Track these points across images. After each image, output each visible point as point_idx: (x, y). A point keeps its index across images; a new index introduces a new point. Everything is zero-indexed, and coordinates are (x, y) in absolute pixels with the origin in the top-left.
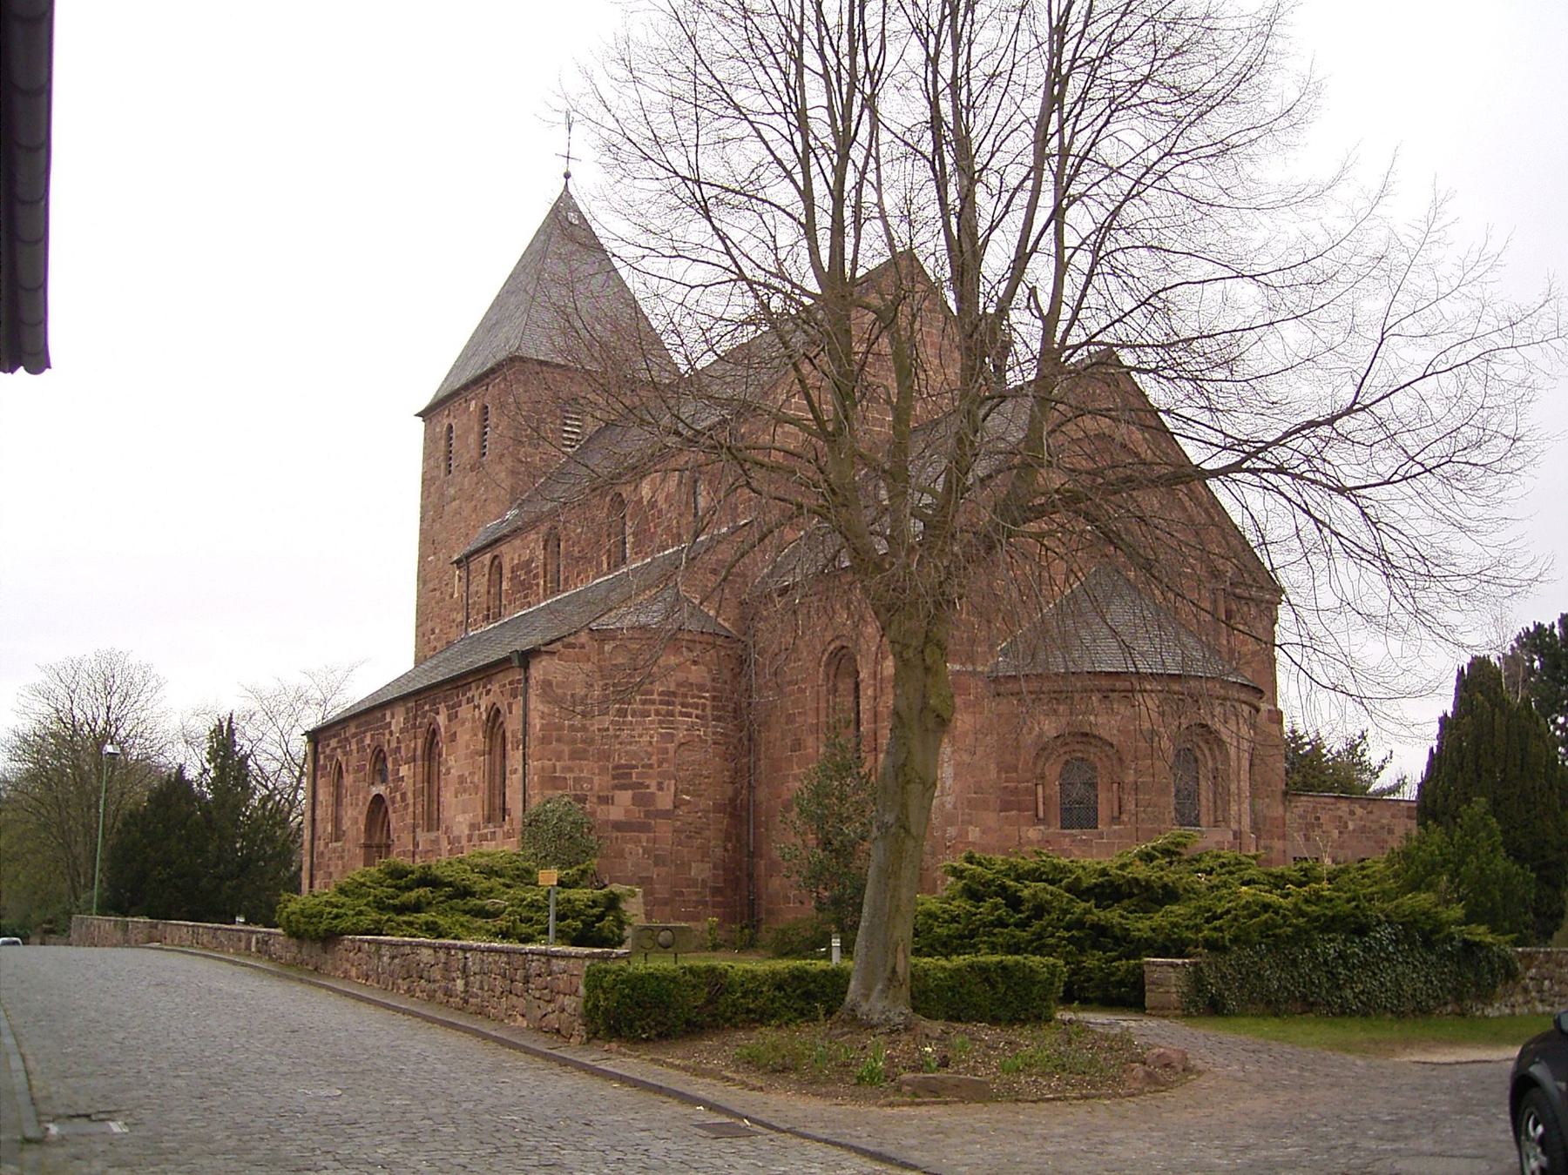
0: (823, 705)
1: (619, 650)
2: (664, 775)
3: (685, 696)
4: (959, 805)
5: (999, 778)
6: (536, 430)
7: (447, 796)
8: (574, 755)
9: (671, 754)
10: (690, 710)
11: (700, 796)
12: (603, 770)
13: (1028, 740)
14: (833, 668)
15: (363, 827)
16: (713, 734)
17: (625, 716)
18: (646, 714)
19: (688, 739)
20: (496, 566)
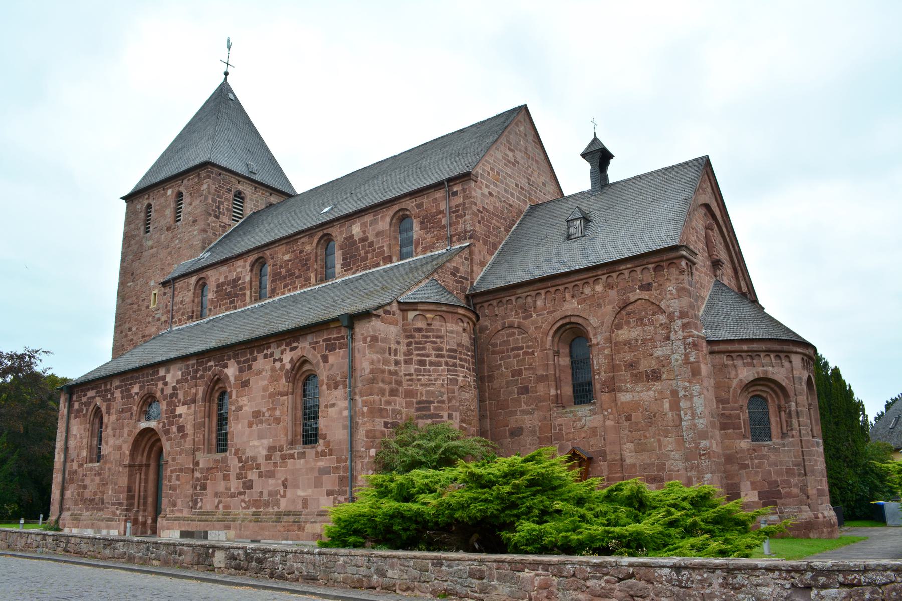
0: (551, 362)
1: (420, 316)
5: (718, 407)
6: (219, 208)
7: (237, 429)
8: (394, 392)
11: (470, 424)
12: (409, 405)
13: (735, 382)
14: (556, 339)
15: (127, 453)
16: (474, 380)
17: (425, 365)
18: (439, 364)
19: (464, 383)
20: (202, 285)
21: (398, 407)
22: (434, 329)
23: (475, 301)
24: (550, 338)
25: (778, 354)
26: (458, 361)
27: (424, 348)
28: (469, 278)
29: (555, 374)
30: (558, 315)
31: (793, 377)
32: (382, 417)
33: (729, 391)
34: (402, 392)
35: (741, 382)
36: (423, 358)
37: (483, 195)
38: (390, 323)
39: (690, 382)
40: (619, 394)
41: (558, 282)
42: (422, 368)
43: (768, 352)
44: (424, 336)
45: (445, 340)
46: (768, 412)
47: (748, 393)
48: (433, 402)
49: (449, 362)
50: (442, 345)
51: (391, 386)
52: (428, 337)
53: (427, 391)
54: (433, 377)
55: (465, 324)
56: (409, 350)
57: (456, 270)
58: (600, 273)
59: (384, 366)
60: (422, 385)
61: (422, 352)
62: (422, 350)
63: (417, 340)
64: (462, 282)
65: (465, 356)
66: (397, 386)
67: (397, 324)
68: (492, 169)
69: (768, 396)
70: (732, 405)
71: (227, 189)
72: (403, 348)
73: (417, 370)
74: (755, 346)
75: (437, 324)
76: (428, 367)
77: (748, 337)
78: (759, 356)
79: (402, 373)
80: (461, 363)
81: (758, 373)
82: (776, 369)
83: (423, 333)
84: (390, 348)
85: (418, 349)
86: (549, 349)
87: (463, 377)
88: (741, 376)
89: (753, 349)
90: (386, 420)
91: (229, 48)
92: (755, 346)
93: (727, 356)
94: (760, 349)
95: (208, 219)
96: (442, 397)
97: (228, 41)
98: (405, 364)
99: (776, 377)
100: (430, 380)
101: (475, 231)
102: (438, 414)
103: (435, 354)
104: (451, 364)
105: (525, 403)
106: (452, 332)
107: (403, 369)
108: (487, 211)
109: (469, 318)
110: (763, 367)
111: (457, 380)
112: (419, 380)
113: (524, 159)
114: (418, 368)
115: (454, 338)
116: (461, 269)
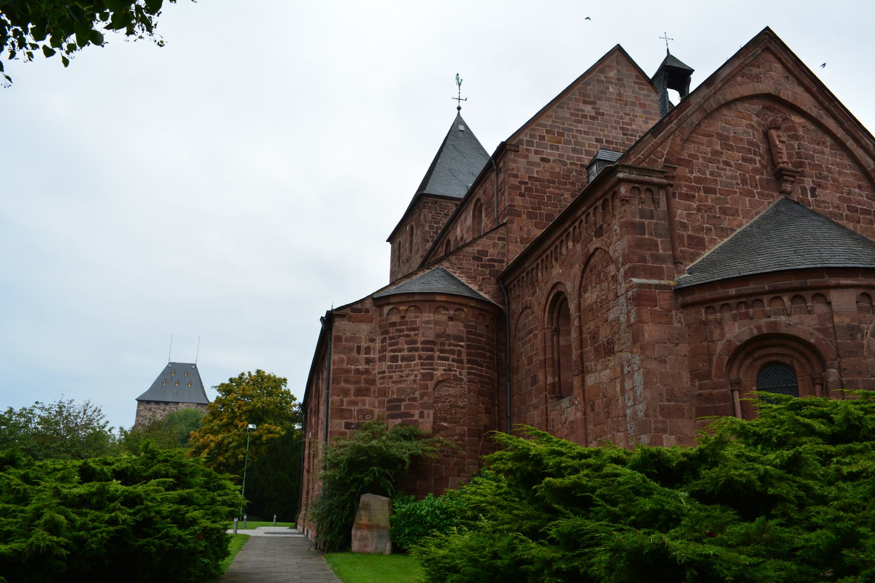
0: (548, 344)
1: (395, 311)
2: (424, 406)
3: (443, 344)
4: (651, 412)
5: (693, 386)
8: (360, 392)
9: (430, 390)
10: (447, 355)
12: (381, 404)
13: (720, 346)
14: (555, 315)
16: (469, 373)
17: (397, 361)
18: (412, 359)
19: (445, 378)
21: (367, 407)
22: (407, 321)
23: (506, 284)
24: (547, 315)
25: (797, 294)
26: (437, 354)
27: (397, 344)
28: (506, 259)
29: (553, 358)
30: (549, 286)
31: (834, 327)
32: (342, 418)
33: (711, 361)
34: (374, 391)
35: (730, 345)
36: (396, 354)
37: (530, 163)
38: (361, 321)
39: (632, 352)
40: (587, 377)
41: (546, 245)
42: (394, 364)
43: (776, 294)
44: (398, 330)
45: (420, 332)
46: (797, 387)
47: (755, 360)
48: (404, 400)
49: (423, 356)
50: (416, 338)
51: (357, 386)
52: (401, 331)
54: (404, 374)
55: (452, 312)
56: (382, 347)
57: (484, 253)
58: (567, 225)
59: (349, 366)
60: (393, 382)
61: (394, 348)
62: (394, 346)
63: (391, 335)
64: (494, 265)
65: (452, 347)
67: (371, 322)
68: (548, 132)
69: (795, 362)
70: (715, 380)
71: (444, 214)
72: (378, 345)
73: (390, 367)
74: (751, 287)
75: (411, 316)
76: (400, 363)
77: (738, 275)
78: (761, 301)
79: (376, 372)
80: (442, 355)
81: (759, 328)
82: (794, 319)
83: (397, 328)
84: (359, 348)
85: (391, 345)
86: (547, 328)
87: (444, 370)
88: (728, 336)
89: (747, 292)
91: (460, 84)
92: (751, 287)
93: (707, 308)
94: (760, 290)
95: (426, 245)
97: (458, 79)
98: (379, 362)
99: (794, 332)
100: (401, 377)
101: (515, 206)
102: (408, 413)
103: (408, 348)
104: (424, 357)
105: (535, 396)
106: (428, 322)
107: (377, 368)
108: (537, 179)
110: (769, 317)
112: (391, 377)
114: (390, 365)
115: (431, 328)
116: (491, 251)
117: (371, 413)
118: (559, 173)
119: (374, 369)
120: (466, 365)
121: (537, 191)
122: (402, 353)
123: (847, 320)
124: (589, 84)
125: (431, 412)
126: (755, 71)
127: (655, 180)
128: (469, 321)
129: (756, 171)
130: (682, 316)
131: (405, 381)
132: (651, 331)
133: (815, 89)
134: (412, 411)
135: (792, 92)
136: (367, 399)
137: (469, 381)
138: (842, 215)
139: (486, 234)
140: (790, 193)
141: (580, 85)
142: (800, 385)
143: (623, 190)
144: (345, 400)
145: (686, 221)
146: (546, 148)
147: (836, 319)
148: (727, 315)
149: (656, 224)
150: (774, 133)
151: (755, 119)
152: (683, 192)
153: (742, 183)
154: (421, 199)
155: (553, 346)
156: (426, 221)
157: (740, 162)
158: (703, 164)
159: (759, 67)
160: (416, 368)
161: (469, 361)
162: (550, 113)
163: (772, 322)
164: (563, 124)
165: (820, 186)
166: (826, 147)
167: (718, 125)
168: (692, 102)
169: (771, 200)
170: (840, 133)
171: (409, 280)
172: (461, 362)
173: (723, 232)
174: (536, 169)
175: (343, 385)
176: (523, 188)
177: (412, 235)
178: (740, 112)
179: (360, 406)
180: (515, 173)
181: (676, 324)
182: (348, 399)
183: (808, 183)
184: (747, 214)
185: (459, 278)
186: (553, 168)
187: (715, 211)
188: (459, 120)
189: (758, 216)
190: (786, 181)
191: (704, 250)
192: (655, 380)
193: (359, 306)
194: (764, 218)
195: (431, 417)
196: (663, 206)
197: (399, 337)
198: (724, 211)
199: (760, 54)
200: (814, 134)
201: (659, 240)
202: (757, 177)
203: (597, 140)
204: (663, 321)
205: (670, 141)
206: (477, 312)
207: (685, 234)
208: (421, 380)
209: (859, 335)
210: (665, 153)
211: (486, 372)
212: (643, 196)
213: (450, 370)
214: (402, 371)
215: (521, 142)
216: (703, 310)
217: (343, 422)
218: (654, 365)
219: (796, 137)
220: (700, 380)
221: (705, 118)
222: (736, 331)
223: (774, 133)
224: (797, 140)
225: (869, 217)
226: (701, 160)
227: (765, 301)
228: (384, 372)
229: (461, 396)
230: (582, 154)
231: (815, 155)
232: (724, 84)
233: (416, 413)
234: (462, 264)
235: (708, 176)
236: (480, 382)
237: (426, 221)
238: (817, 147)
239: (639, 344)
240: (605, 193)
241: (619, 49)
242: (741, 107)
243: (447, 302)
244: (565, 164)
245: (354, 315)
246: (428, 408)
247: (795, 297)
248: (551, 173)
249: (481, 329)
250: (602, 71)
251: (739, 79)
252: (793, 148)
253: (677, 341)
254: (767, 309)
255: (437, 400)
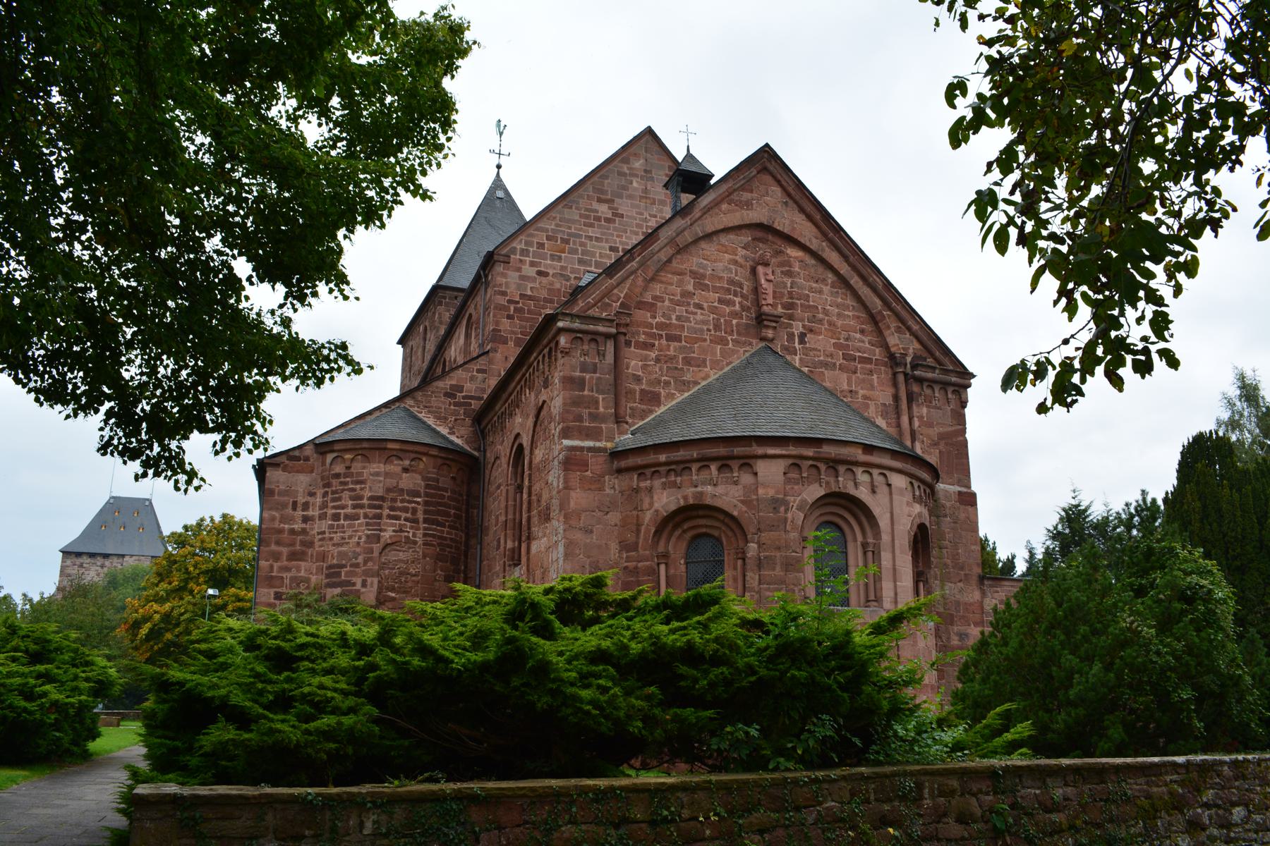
1: (339, 459)
2: (367, 573)
3: (394, 500)
8: (294, 556)
9: (376, 554)
10: (398, 513)
12: (320, 570)
16: (425, 535)
17: (339, 520)
18: (356, 517)
19: (394, 540)
21: (302, 574)
26: (386, 512)
27: (339, 499)
29: (514, 519)
32: (272, 586)
33: (638, 531)
34: (312, 555)
37: (523, 278)
38: (298, 472)
47: (684, 532)
48: (344, 566)
50: (362, 493)
52: (345, 483)
53: (339, 553)
54: (346, 535)
56: (323, 502)
57: (459, 388)
60: (334, 545)
66: (304, 549)
67: (312, 472)
69: (723, 535)
72: (319, 500)
73: (331, 527)
75: (357, 467)
76: (342, 522)
79: (315, 532)
81: (685, 498)
84: (295, 504)
85: (334, 500)
87: (394, 531)
88: (657, 505)
89: (676, 459)
90: (280, 590)
92: (681, 454)
96: (356, 559)
100: (343, 538)
101: (500, 331)
102: (349, 581)
104: (370, 515)
106: (377, 474)
108: (530, 298)
109: (416, 452)
111: (378, 537)
112: (331, 539)
113: (638, 207)
115: (380, 482)
116: (468, 386)
117: (307, 580)
118: (559, 290)
119: (312, 529)
120: (422, 525)
121: (530, 312)
122: (345, 511)
123: (771, 493)
124: (607, 177)
125: (376, 580)
126: (746, 196)
127: (601, 329)
128: (429, 473)
129: (734, 315)
130: (616, 481)
131: (348, 543)
132: (578, 498)
133: (818, 217)
134: (354, 580)
135: (790, 220)
136: (303, 564)
137: (424, 544)
138: (835, 364)
139: (461, 366)
140: (772, 340)
141: (596, 178)
142: (726, 559)
143: (563, 340)
144: (276, 565)
145: (640, 373)
146: (546, 259)
147: (761, 491)
148: (657, 483)
149: (599, 379)
150: (760, 269)
151: (742, 252)
152: (641, 340)
153: (715, 329)
154: (436, 291)
155: (515, 505)
156: (441, 323)
157: (716, 304)
158: (669, 307)
159: (752, 191)
160: (360, 529)
161: (425, 521)
162: (553, 214)
163: (698, 493)
164: (570, 228)
165: (811, 331)
166: (827, 285)
167: (694, 261)
168: (661, 235)
169: (748, 348)
170: (844, 269)
171: (362, 421)
172: (415, 521)
173: (684, 385)
174: (530, 285)
175: (274, 547)
176: (512, 308)
177: (425, 339)
178: (723, 245)
179: (293, 573)
180: (503, 289)
181: (608, 491)
182: (279, 564)
183: (797, 328)
184: (716, 365)
185: (426, 419)
186: (552, 284)
187: (678, 362)
188: (498, 184)
189: (730, 367)
190: (767, 327)
191: (659, 405)
192: (577, 552)
193: (297, 453)
194: (734, 370)
195: (376, 586)
196: (610, 358)
197: (343, 491)
198: (687, 361)
199: (755, 176)
200: (812, 270)
201: (601, 397)
202: (734, 322)
203: (612, 249)
204: (593, 487)
205: (629, 281)
206: (440, 461)
207: (637, 388)
208: (366, 543)
209: (782, 509)
210: (622, 296)
211: (448, 533)
212: (586, 347)
213: (401, 531)
214: (344, 532)
215: (514, 251)
216: (636, 476)
217: (272, 591)
218: (578, 536)
219: (789, 274)
220: (627, 552)
221: (679, 252)
222: (665, 500)
223: (760, 269)
224: (791, 277)
225: (869, 366)
226: (667, 303)
227: (693, 469)
228: (324, 533)
229: (413, 562)
230: (591, 266)
231: (811, 294)
232: (705, 213)
233: (359, 581)
234: (429, 402)
235: (674, 321)
236: (439, 544)
237: (441, 323)
238: (814, 285)
239: (563, 512)
240: (550, 342)
241: (649, 132)
242: (724, 239)
243: (401, 450)
244: (568, 279)
245: (291, 463)
246: (373, 576)
247: (723, 466)
248: (549, 289)
249: (445, 482)
250: (626, 161)
251: (724, 206)
252: (785, 287)
253: (607, 510)
254: (695, 477)
255: (383, 566)
